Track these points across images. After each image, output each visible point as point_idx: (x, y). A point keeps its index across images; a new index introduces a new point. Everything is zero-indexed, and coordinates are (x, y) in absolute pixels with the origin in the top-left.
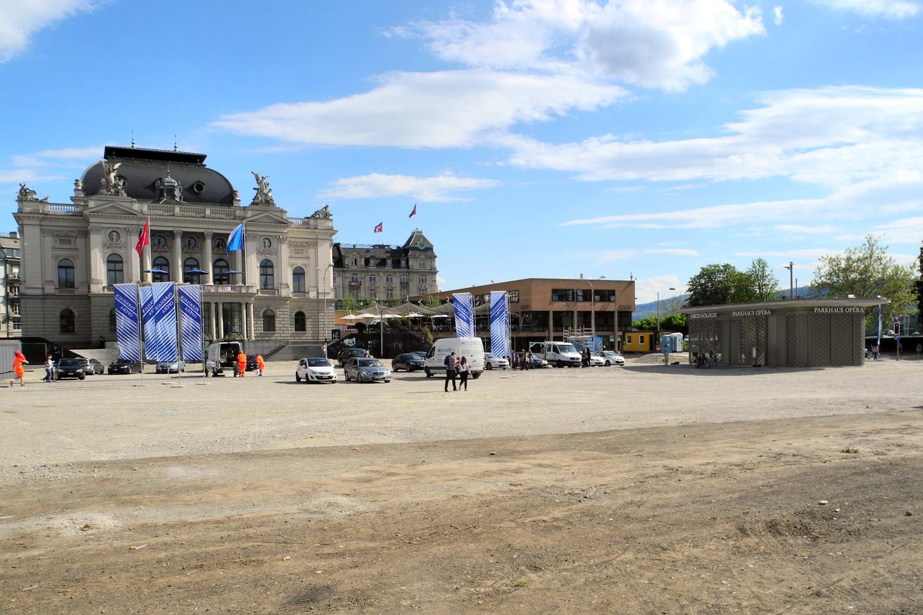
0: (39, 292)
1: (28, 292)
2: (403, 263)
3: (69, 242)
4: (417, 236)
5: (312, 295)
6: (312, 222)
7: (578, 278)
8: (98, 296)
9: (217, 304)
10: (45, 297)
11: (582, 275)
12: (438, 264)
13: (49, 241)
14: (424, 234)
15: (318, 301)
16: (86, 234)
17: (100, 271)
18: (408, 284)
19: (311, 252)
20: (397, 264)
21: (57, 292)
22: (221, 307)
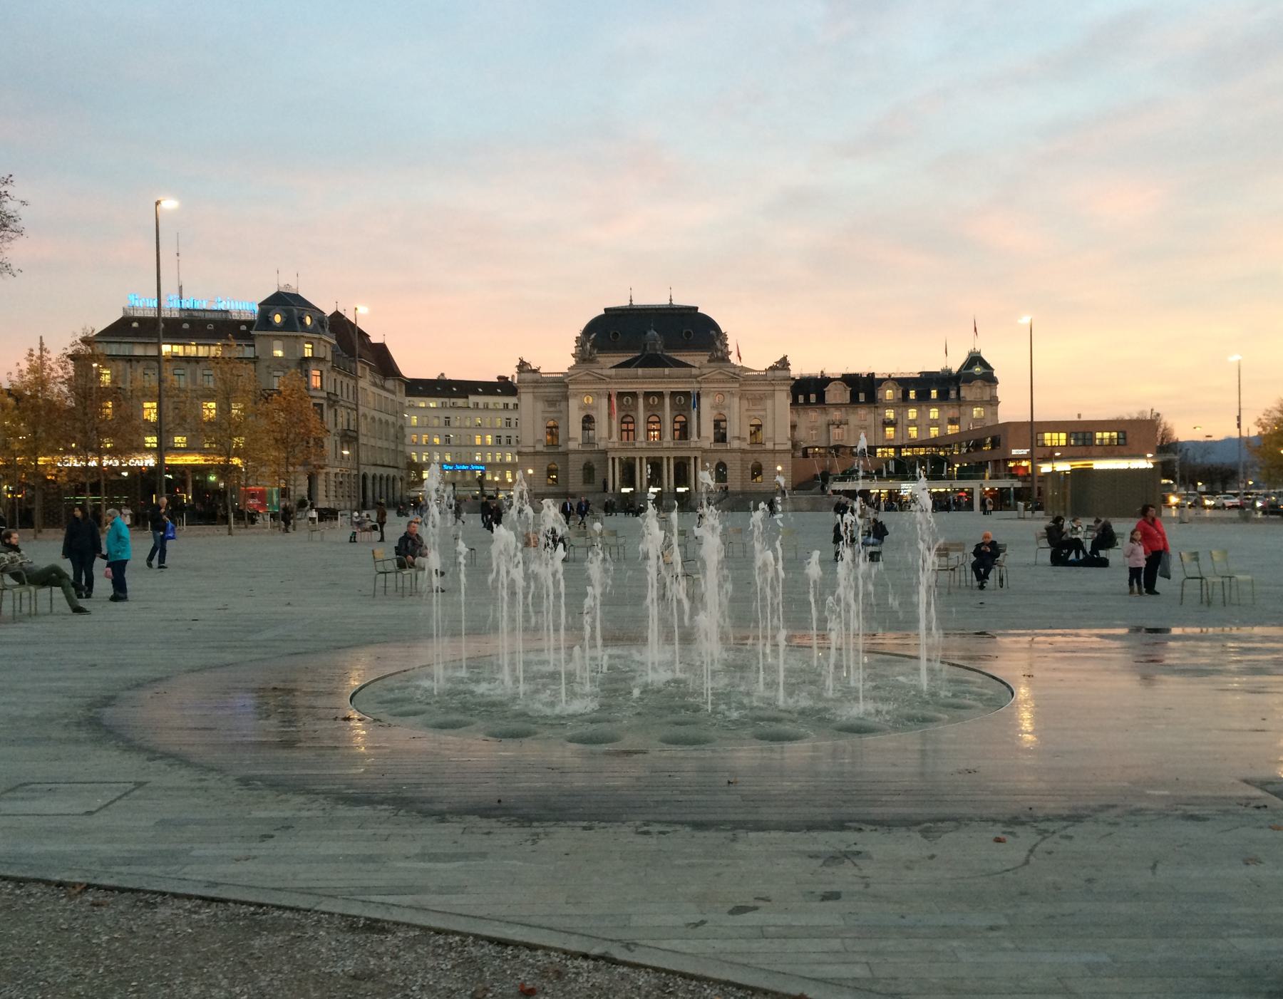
0: (531, 450)
1: (525, 450)
2: (953, 394)
3: (554, 405)
4: (975, 359)
5: (769, 446)
6: (770, 373)
7: (1076, 419)
8: (576, 452)
9: (668, 458)
10: (536, 453)
11: (1079, 416)
12: (1001, 391)
13: (540, 406)
14: (983, 355)
15: (774, 451)
16: (566, 398)
17: (575, 429)
18: (958, 419)
19: (769, 403)
20: (944, 396)
21: (545, 450)
22: (672, 462)
